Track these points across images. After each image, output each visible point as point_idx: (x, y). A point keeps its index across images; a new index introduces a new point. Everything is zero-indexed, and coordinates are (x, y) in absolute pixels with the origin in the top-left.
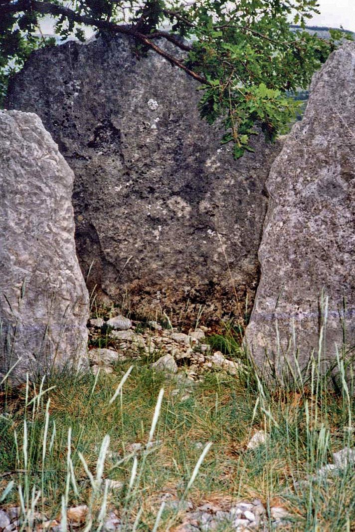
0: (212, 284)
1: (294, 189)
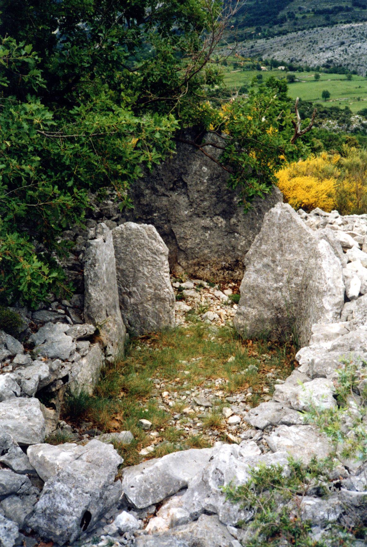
0: (237, 261)
1: (254, 265)
